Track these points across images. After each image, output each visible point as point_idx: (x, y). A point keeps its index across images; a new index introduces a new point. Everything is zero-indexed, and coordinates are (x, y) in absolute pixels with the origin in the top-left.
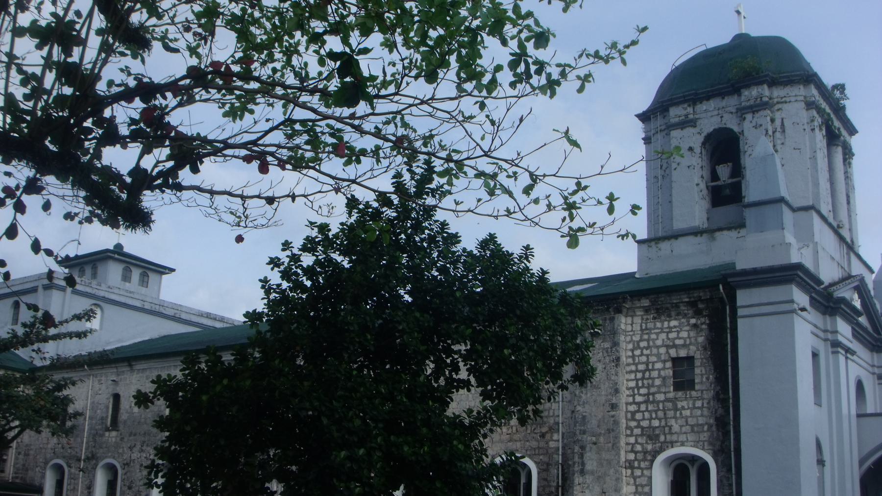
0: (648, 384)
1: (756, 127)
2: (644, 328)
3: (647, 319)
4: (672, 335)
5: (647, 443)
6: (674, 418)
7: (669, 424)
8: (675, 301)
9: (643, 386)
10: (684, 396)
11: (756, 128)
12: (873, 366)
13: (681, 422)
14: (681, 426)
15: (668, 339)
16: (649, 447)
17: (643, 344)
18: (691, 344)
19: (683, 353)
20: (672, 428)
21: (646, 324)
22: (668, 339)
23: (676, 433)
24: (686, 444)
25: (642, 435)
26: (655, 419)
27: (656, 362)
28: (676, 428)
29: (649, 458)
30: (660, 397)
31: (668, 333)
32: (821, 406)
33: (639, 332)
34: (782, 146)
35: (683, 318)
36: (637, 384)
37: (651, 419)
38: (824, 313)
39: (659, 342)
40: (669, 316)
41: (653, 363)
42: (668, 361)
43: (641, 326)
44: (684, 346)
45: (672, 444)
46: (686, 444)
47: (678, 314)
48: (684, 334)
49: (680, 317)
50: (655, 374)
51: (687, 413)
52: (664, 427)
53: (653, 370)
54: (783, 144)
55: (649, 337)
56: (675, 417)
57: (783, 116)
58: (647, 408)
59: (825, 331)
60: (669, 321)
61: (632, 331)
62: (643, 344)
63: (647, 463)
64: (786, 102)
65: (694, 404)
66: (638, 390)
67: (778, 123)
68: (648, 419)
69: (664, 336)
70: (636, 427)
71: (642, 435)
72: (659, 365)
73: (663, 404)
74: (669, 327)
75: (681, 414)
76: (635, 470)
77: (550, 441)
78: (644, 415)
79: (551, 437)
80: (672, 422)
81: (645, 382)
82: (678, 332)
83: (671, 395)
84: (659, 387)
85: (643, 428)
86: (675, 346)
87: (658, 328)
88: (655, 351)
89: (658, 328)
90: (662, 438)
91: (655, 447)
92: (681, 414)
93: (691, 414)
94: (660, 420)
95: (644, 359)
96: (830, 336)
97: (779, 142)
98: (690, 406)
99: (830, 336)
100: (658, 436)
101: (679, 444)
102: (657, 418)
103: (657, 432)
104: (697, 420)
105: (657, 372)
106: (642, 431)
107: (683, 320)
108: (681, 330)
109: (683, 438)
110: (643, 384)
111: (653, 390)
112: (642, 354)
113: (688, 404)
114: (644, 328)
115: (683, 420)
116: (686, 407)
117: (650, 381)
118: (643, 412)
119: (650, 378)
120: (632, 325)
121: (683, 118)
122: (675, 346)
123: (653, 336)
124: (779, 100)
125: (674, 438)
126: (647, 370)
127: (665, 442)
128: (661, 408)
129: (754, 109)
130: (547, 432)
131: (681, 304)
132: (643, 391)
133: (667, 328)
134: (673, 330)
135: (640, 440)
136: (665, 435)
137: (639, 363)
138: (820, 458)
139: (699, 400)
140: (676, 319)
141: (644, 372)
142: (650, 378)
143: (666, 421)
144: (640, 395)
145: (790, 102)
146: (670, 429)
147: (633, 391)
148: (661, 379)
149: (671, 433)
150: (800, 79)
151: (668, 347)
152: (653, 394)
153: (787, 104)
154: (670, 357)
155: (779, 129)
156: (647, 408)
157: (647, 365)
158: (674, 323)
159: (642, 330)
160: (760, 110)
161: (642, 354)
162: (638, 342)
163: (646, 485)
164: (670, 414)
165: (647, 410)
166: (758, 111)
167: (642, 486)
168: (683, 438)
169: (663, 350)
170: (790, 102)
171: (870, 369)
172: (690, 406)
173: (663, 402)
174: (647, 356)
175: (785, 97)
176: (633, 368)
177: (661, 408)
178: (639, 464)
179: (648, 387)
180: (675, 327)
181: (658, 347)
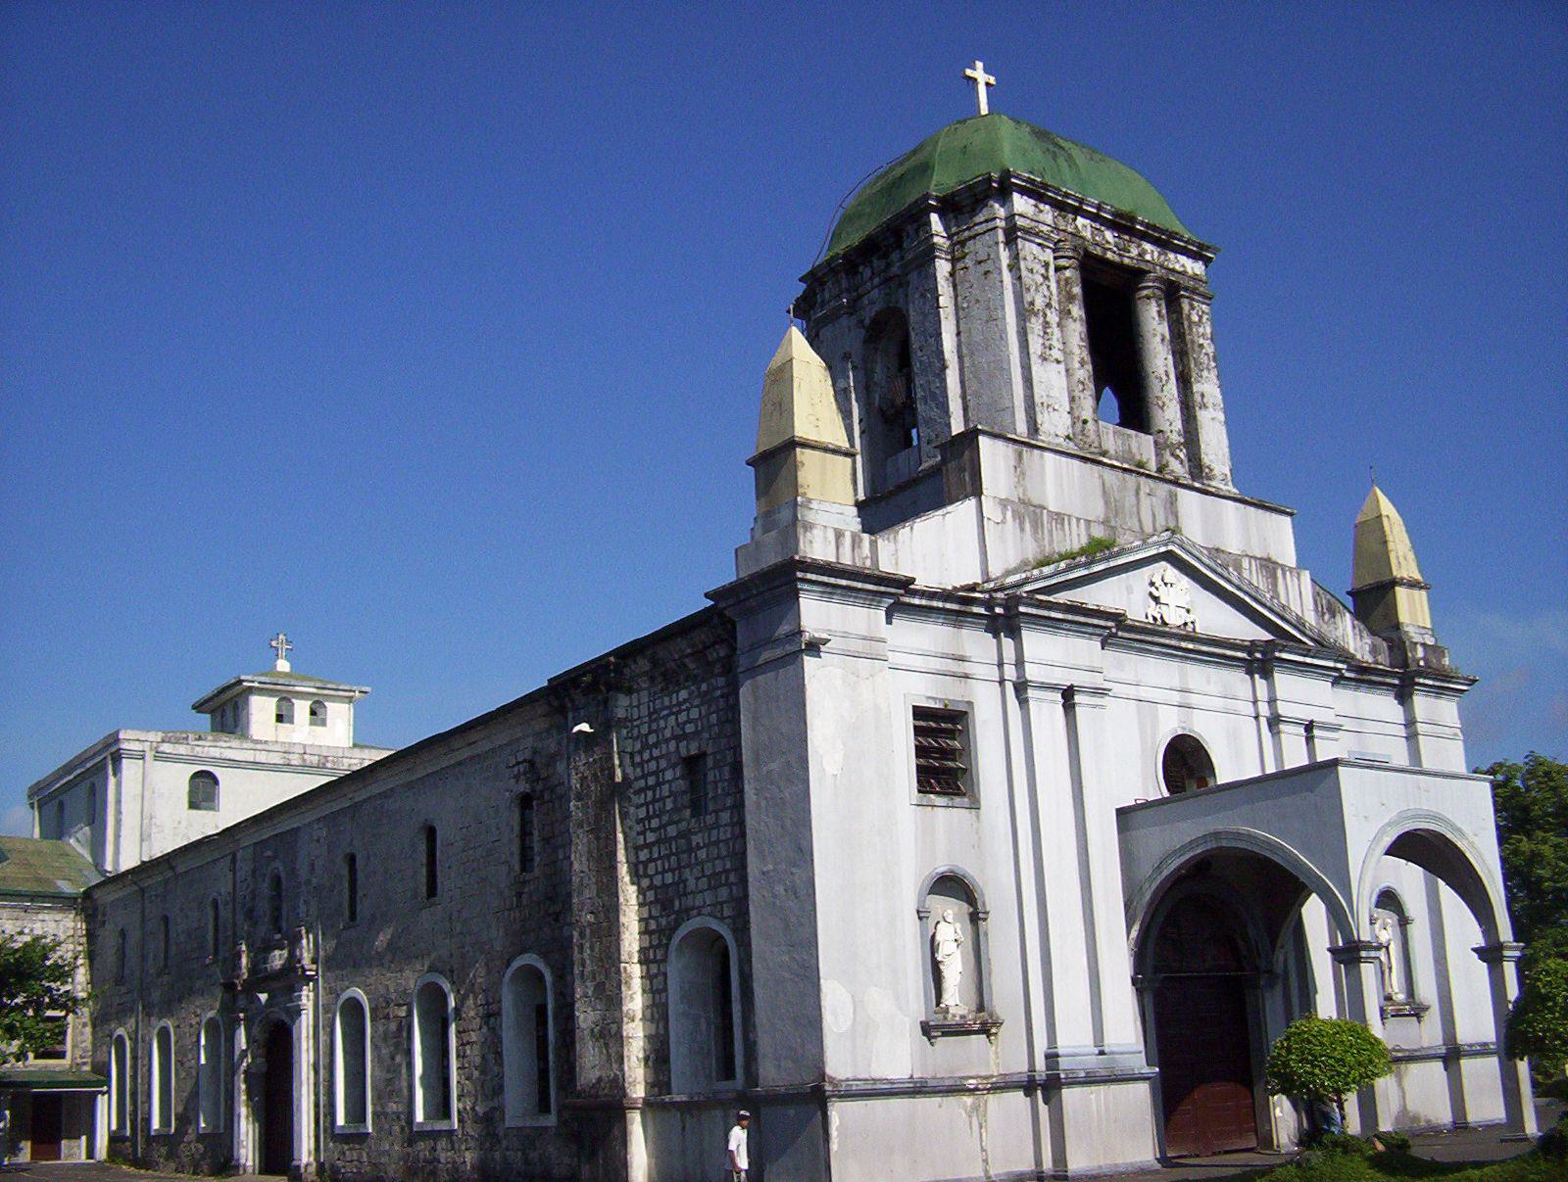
3: (655, 693)
4: (683, 717)
5: (662, 916)
7: (683, 878)
13: (696, 871)
14: (697, 879)
17: (652, 739)
20: (688, 883)
28: (691, 884)
30: (672, 831)
31: (680, 712)
39: (668, 733)
40: (678, 683)
43: (649, 708)
44: (697, 733)
49: (690, 683)
53: (664, 783)
60: (677, 692)
73: (676, 842)
82: (688, 709)
95: (653, 765)
100: (672, 902)
101: (695, 911)
105: (667, 786)
107: (692, 688)
112: (652, 758)
123: (662, 723)
132: (655, 823)
134: (683, 707)
139: (714, 828)
146: (685, 886)
149: (685, 894)
154: (680, 757)
158: (683, 694)
169: (672, 745)
173: (675, 838)
174: (657, 759)
176: (642, 783)
177: (674, 851)
180: (685, 701)
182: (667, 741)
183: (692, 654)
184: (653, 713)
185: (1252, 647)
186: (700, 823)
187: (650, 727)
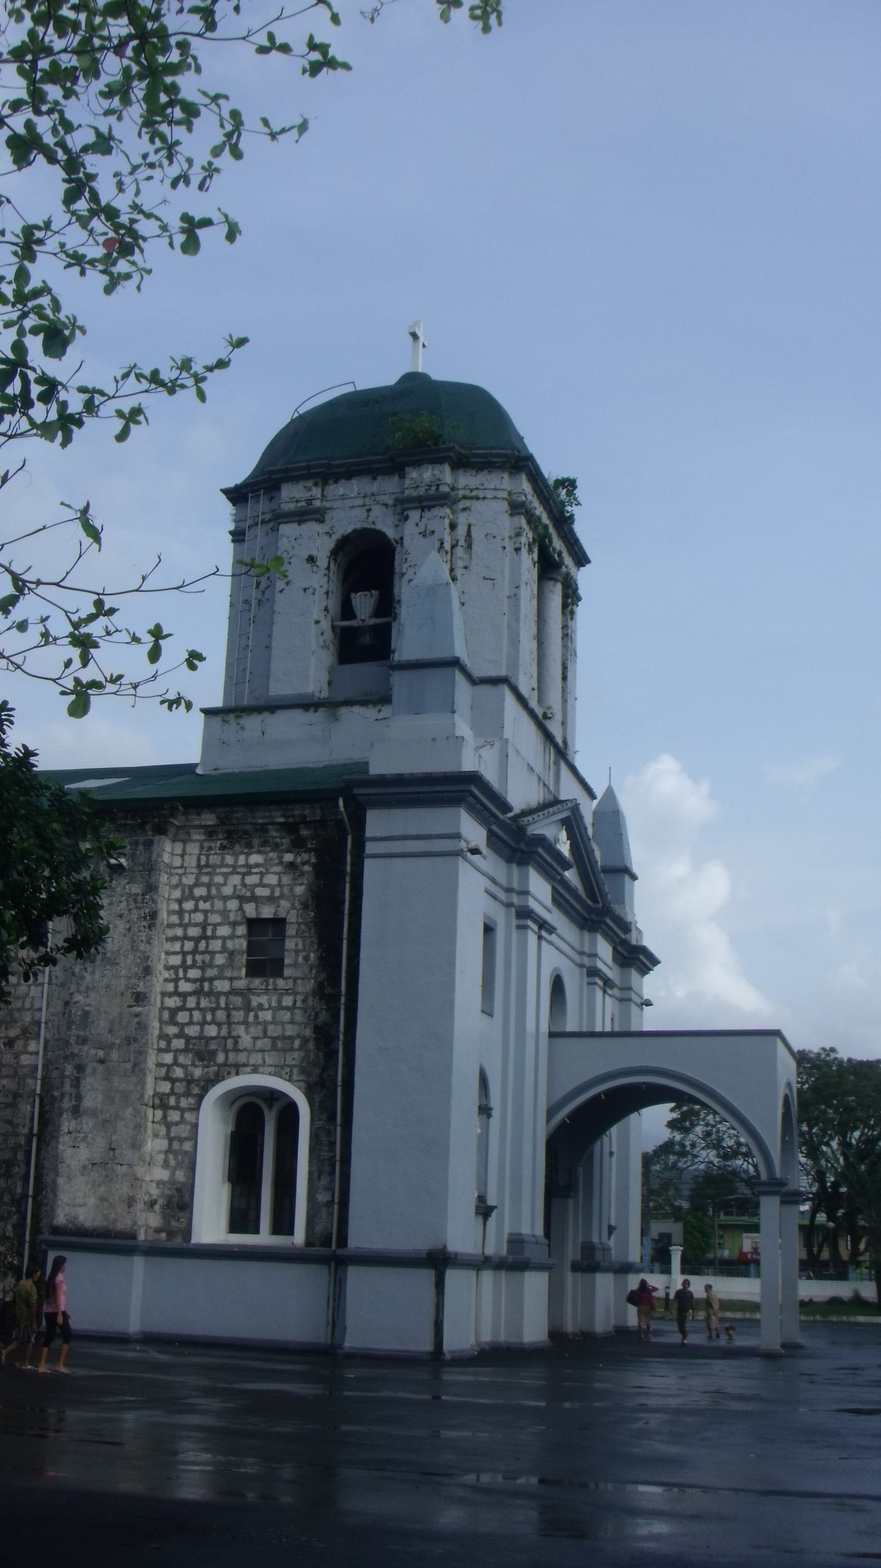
0: (203, 962)
1: (424, 534)
2: (203, 863)
3: (210, 848)
4: (251, 880)
5: (193, 1065)
6: (243, 1023)
7: (234, 1034)
8: (260, 821)
9: (194, 966)
10: (263, 987)
11: (424, 536)
12: (582, 953)
13: (256, 1031)
14: (255, 1039)
15: (244, 885)
16: (198, 1073)
17: (199, 892)
18: (282, 896)
19: (267, 912)
20: (240, 1040)
21: (208, 856)
22: (244, 885)
23: (245, 1050)
24: (261, 1069)
25: (186, 1050)
26: (210, 1024)
27: (219, 924)
28: (246, 1041)
29: (196, 1091)
31: (244, 875)
32: (492, 1016)
33: (195, 871)
34: (464, 571)
35: (272, 851)
36: (184, 961)
37: (203, 1023)
38: (509, 860)
39: (228, 890)
40: (249, 846)
41: (215, 926)
42: (241, 924)
43: (199, 860)
44: (271, 899)
45: (237, 1068)
46: (261, 1069)
47: (264, 844)
48: (272, 879)
49: (268, 849)
50: (216, 945)
51: (267, 1016)
52: (225, 1038)
53: (214, 937)
54: (466, 568)
55: (211, 880)
56: (245, 1023)
57: (472, 520)
58: (198, 1003)
59: (509, 890)
60: (248, 855)
61: (182, 867)
62: (199, 892)
63: (191, 1100)
64: (478, 498)
65: (279, 1002)
66: (185, 972)
67: (461, 531)
68: (198, 1023)
69: (236, 880)
70: (177, 1036)
71: (186, 1050)
72: (224, 931)
73: (227, 999)
74: (247, 866)
75: (256, 1017)
76: (170, 1112)
77: (22, 1053)
78: (191, 1015)
79: (25, 1046)
80: (240, 1030)
81: (199, 958)
82: (262, 875)
83: (241, 984)
84: (221, 968)
85: (188, 1039)
86: (254, 899)
87: (227, 866)
88: (219, 905)
89: (227, 866)
90: (221, 1058)
91: (207, 1073)
92: (256, 1017)
93: (274, 1017)
94: (219, 1025)
95: (199, 917)
96: (515, 899)
97: (460, 564)
98: (274, 1004)
99: (515, 899)
100: (213, 1053)
101: (249, 1069)
102: (214, 1022)
103: (213, 1046)
104: (284, 1029)
106: (187, 1043)
107: (271, 854)
108: (268, 872)
109: (256, 1059)
110: (194, 961)
111: (210, 973)
112: (196, 909)
113: (269, 1001)
114: (203, 863)
115: (260, 1027)
116: (266, 1006)
117: (207, 958)
118: (191, 1010)
119: (206, 952)
120: (182, 856)
121: (303, 504)
122: (254, 899)
123: (219, 879)
124: (468, 493)
125: (242, 1058)
126: (204, 937)
127: (225, 1064)
128: (223, 1005)
129: (424, 504)
130: (17, 1037)
131: (270, 827)
132: (193, 974)
133: (243, 866)
135: (182, 1059)
136: (226, 1051)
137: (190, 924)
138: (484, 1102)
139: (289, 994)
140: (259, 852)
141: (197, 940)
142: (206, 952)
143: (229, 1028)
144: (188, 980)
145: (484, 498)
147: (176, 973)
148: (226, 955)
149: (236, 1050)
150: (505, 463)
151: (242, 899)
152: (211, 980)
153: (480, 501)
154: (244, 917)
155: (462, 542)
156: (198, 1003)
157: (204, 929)
158: (256, 858)
159: (199, 866)
160: (434, 506)
161: (196, 909)
162: (191, 888)
163: (186, 1139)
164: (238, 1016)
165: (198, 1007)
166: (430, 508)
167: (181, 1140)
168: (256, 1059)
169: (233, 905)
170: (484, 498)
171: (576, 957)
172: (274, 1004)
173: (227, 994)
174: (205, 912)
175: (477, 489)
176: (179, 932)
177: (223, 1005)
178: (178, 1101)
179: (203, 968)
180: (257, 865)
181: (225, 899)
182: (225, 899)
183: (281, 824)
184: (207, 865)
186: (268, 985)
187: (197, 879)
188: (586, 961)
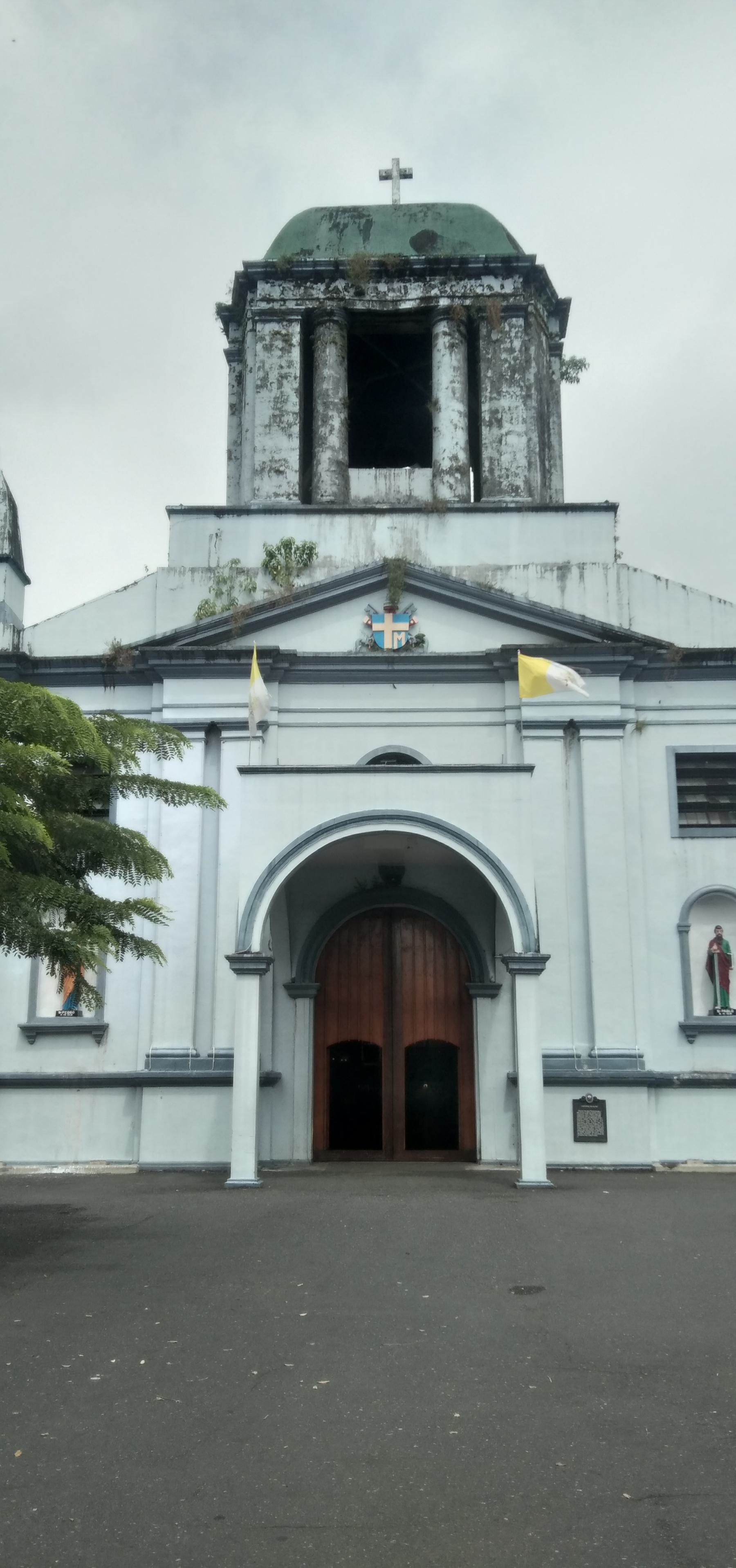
171: (496, 717)
185: (487, 657)
188: (511, 715)
